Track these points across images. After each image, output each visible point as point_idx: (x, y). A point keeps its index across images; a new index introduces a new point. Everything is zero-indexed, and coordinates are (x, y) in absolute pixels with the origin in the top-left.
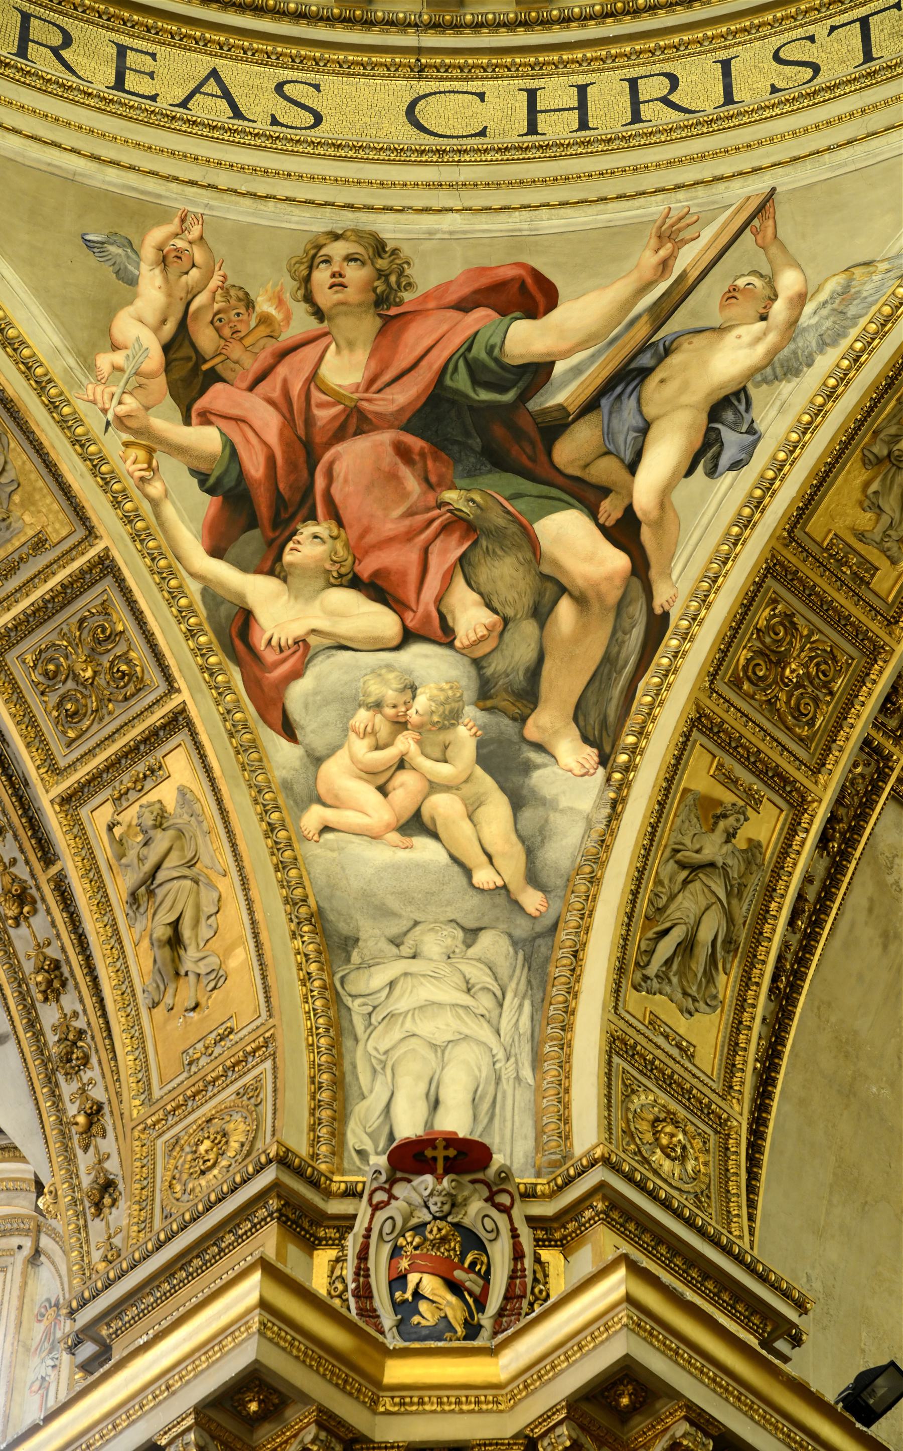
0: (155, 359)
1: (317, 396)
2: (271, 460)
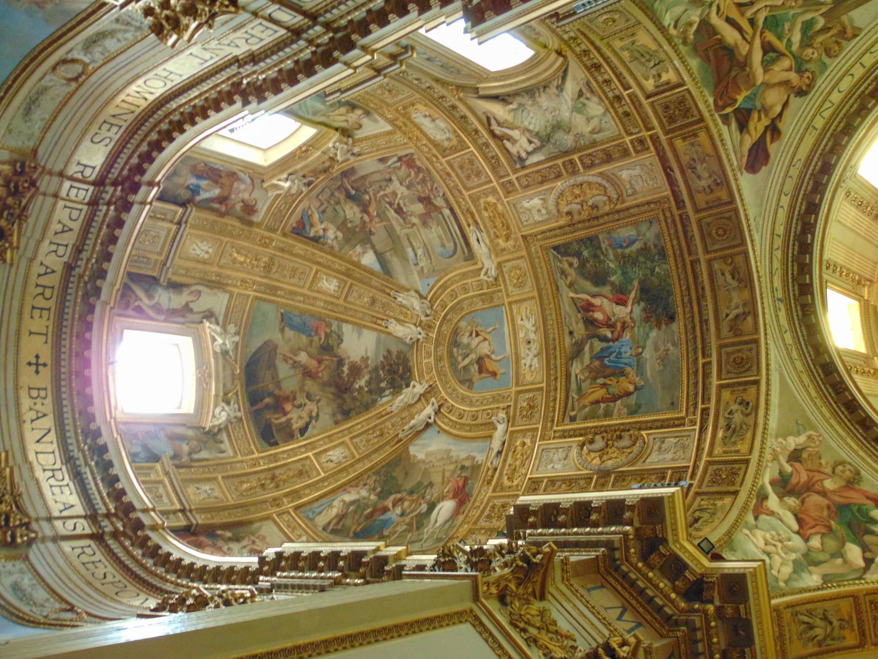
0: (792, 448)
1: (819, 483)
2: (798, 483)
